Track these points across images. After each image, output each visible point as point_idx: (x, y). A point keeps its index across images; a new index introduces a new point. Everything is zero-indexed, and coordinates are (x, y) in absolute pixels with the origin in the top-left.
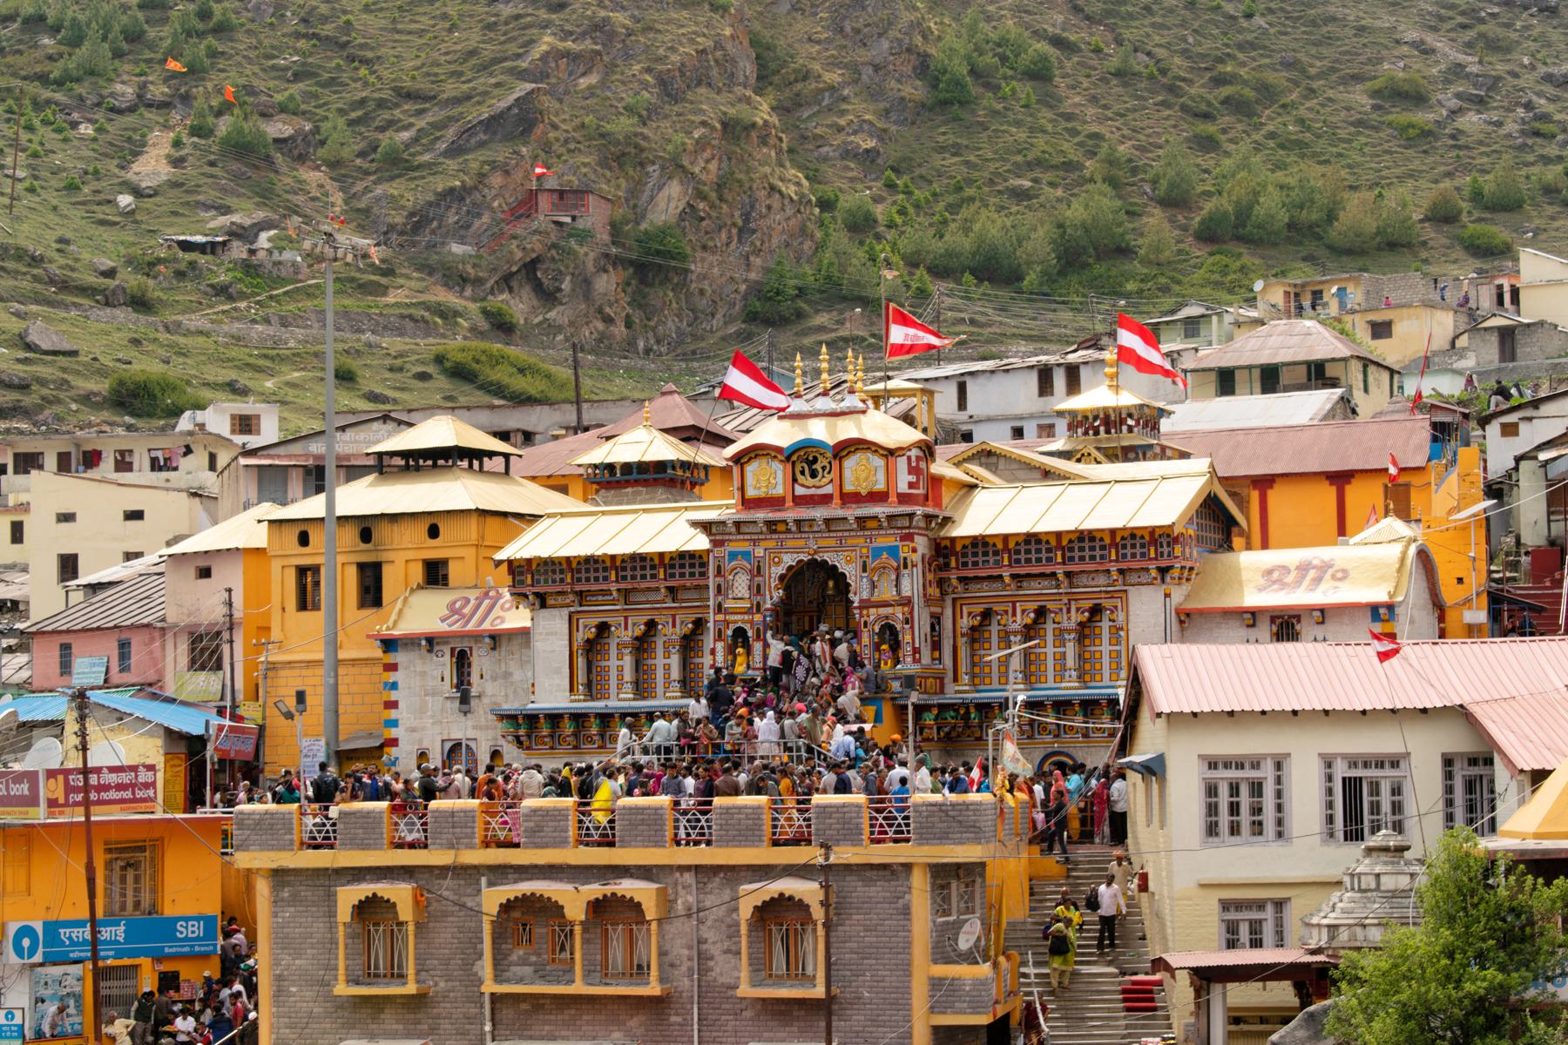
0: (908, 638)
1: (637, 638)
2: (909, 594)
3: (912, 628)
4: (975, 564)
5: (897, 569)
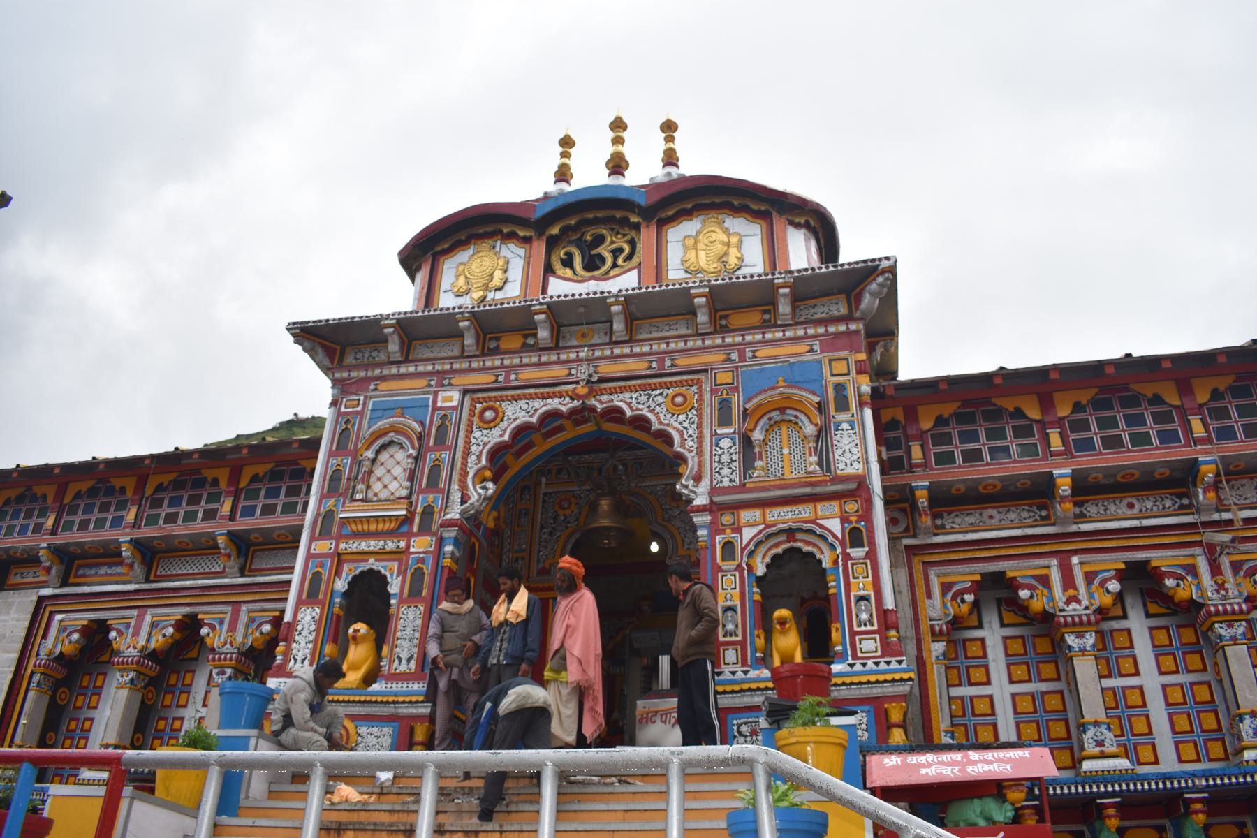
0: (862, 585)
1: (153, 655)
2: (857, 469)
3: (872, 555)
4: (972, 457)
5: (820, 407)
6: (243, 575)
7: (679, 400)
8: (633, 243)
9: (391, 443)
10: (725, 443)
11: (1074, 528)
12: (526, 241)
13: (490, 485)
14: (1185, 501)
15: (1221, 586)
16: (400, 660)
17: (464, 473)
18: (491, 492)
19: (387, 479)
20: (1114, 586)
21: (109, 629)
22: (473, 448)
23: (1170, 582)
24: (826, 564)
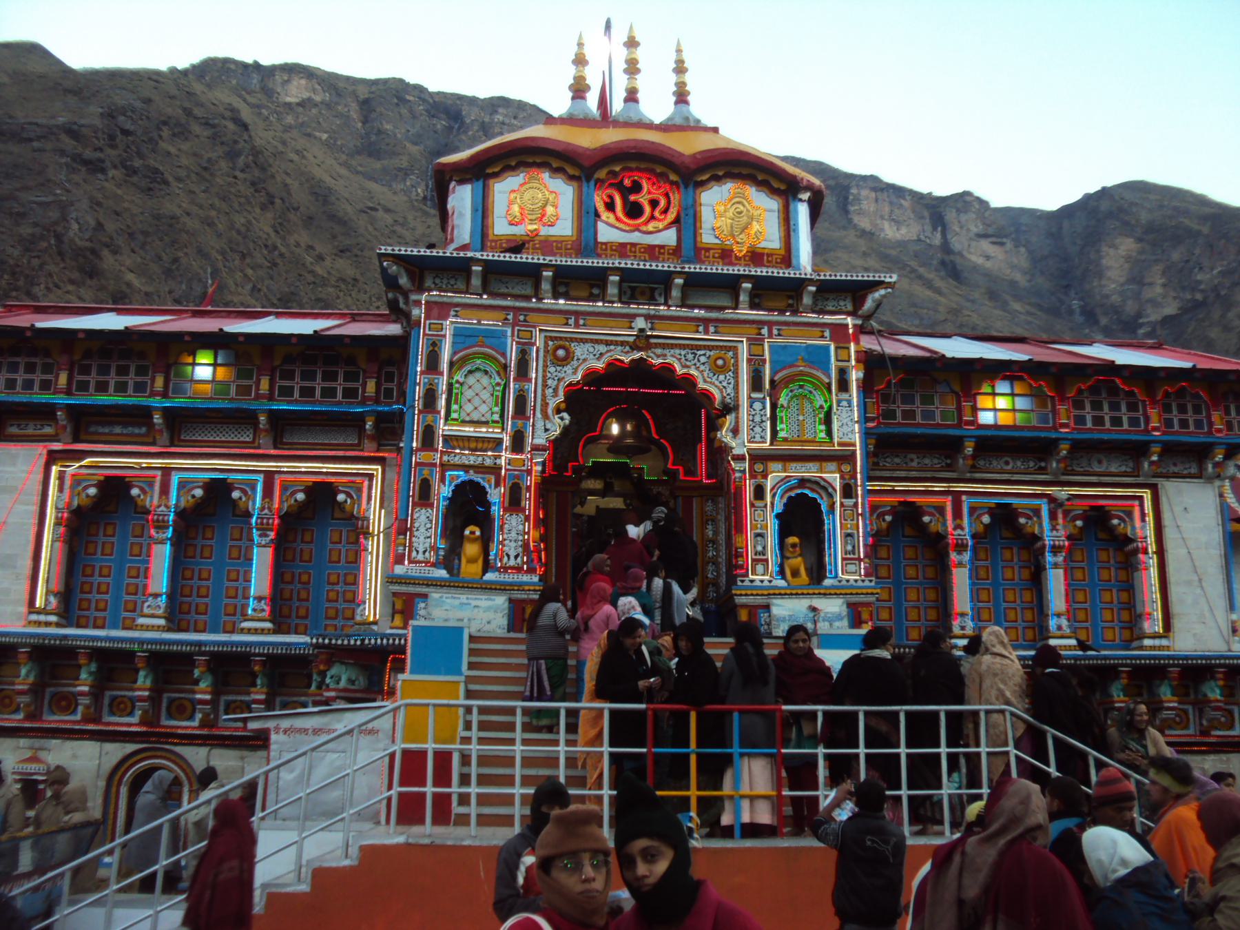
6: (275, 448)
7: (720, 362)
8: (667, 196)
9: (478, 369)
10: (757, 406)
11: (968, 475)
12: (571, 178)
13: (565, 415)
14: (1043, 464)
15: (1054, 528)
16: (508, 556)
17: (545, 405)
18: (567, 422)
19: (477, 401)
20: (986, 519)
21: (129, 486)
22: (549, 382)
23: (1022, 520)
24: (824, 508)
